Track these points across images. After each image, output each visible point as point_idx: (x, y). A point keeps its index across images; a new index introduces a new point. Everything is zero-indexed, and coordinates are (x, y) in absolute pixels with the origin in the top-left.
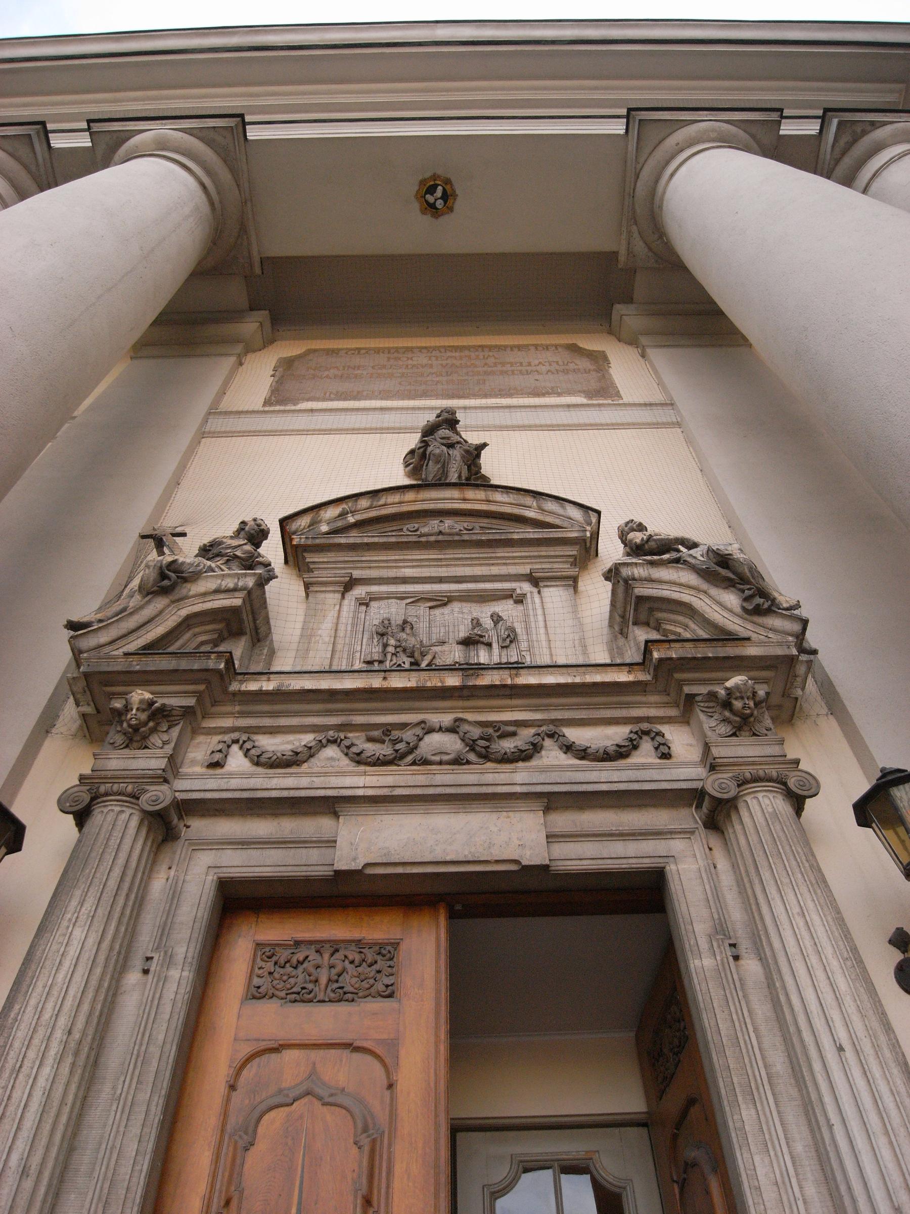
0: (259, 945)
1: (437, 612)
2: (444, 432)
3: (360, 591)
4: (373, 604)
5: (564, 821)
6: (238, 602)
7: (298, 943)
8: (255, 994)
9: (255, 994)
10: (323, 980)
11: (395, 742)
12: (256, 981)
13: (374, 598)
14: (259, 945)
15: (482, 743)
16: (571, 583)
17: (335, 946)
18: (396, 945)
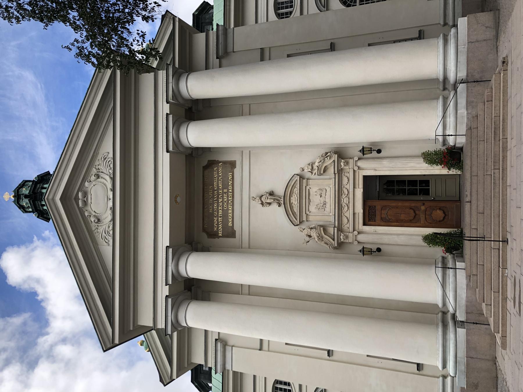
0: (369, 221)
1: (311, 201)
2: (263, 199)
3: (307, 212)
4: (310, 210)
5: (357, 186)
6: (322, 228)
7: (369, 217)
8: (375, 221)
9: (375, 221)
10: (373, 214)
11: (345, 206)
12: (373, 221)
13: (309, 211)
14: (369, 221)
15: (346, 195)
16: (308, 180)
17: (369, 213)
18: (369, 206)
